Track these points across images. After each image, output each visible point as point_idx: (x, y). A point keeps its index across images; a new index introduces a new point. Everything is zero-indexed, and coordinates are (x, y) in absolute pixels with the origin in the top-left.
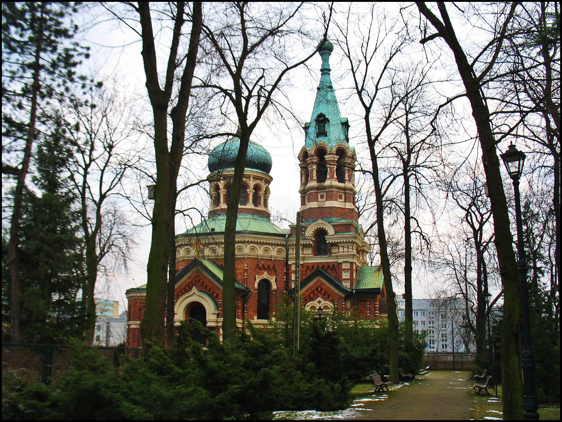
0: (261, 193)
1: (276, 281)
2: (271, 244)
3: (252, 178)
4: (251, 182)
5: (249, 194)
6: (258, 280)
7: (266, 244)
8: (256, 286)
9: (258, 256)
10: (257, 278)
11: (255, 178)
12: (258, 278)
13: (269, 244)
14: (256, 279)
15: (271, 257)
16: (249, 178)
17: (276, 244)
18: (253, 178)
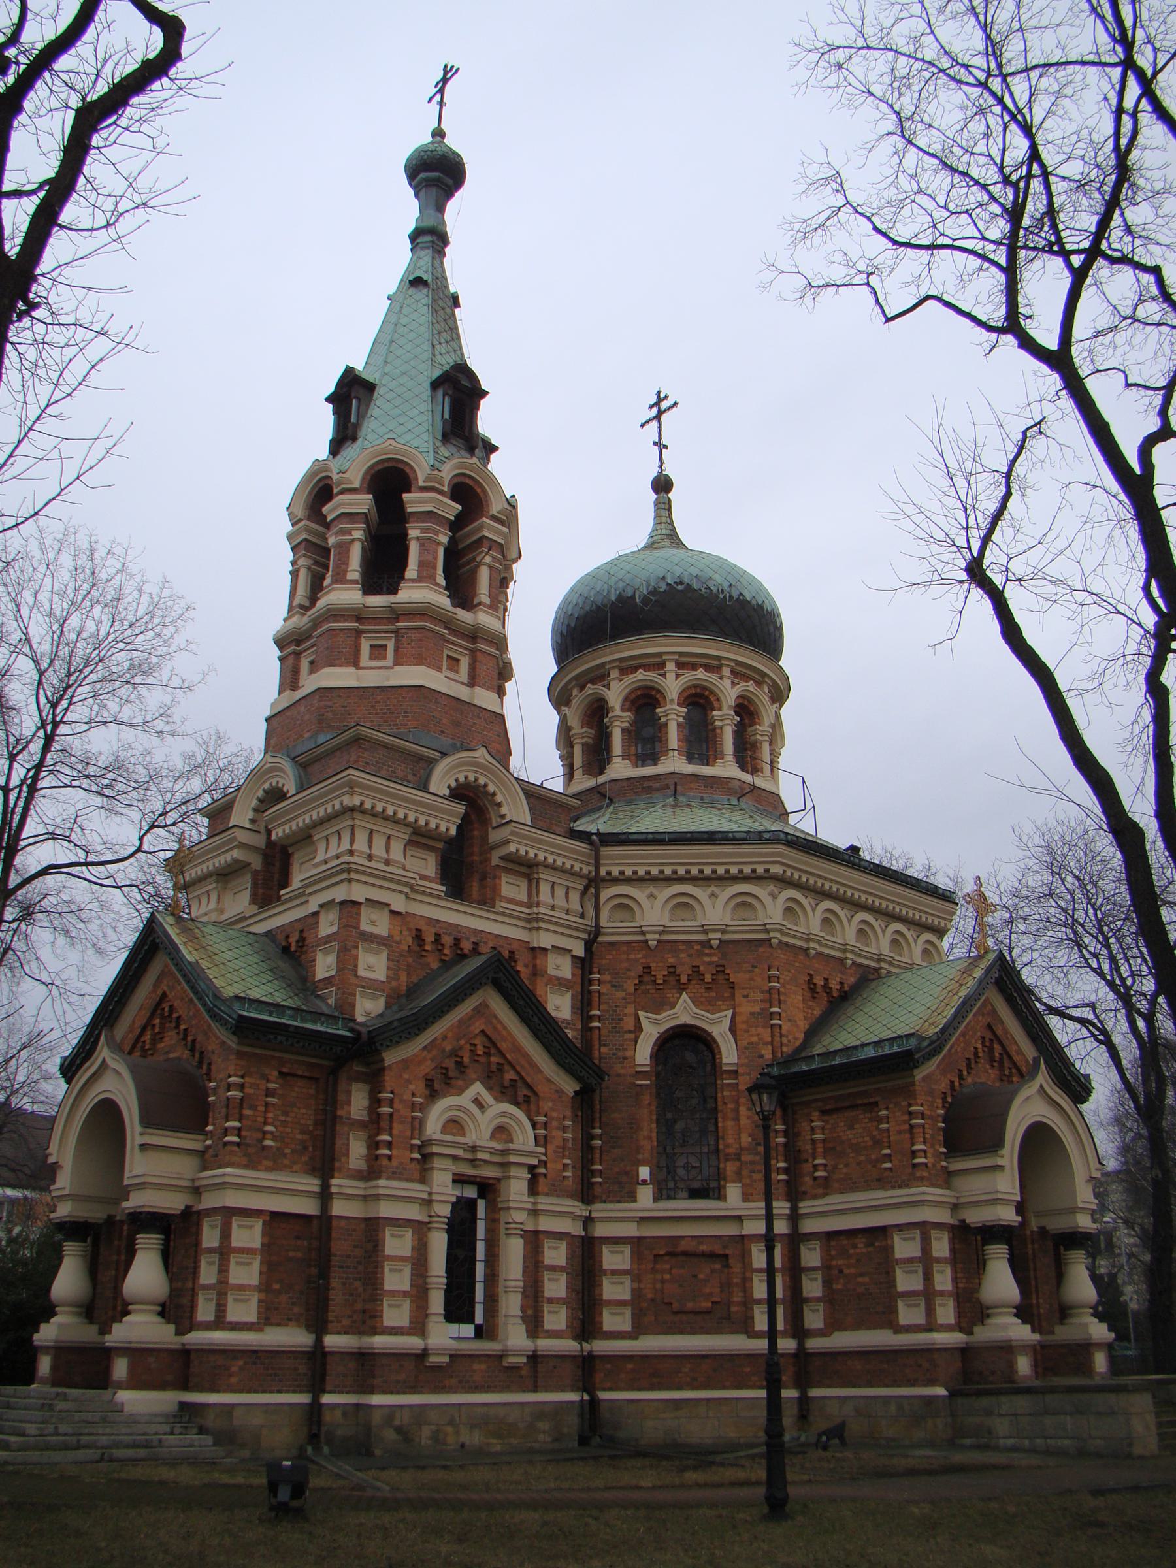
0: (725, 720)
1: (733, 1029)
2: (701, 879)
3: (671, 666)
4: (671, 676)
5: (666, 725)
6: (652, 1029)
7: (676, 879)
8: (643, 1054)
9: (643, 933)
10: (645, 1023)
11: (683, 665)
12: (654, 1022)
13: (688, 879)
14: (639, 1028)
15: (706, 932)
16: (661, 666)
17: (720, 879)
18: (680, 666)
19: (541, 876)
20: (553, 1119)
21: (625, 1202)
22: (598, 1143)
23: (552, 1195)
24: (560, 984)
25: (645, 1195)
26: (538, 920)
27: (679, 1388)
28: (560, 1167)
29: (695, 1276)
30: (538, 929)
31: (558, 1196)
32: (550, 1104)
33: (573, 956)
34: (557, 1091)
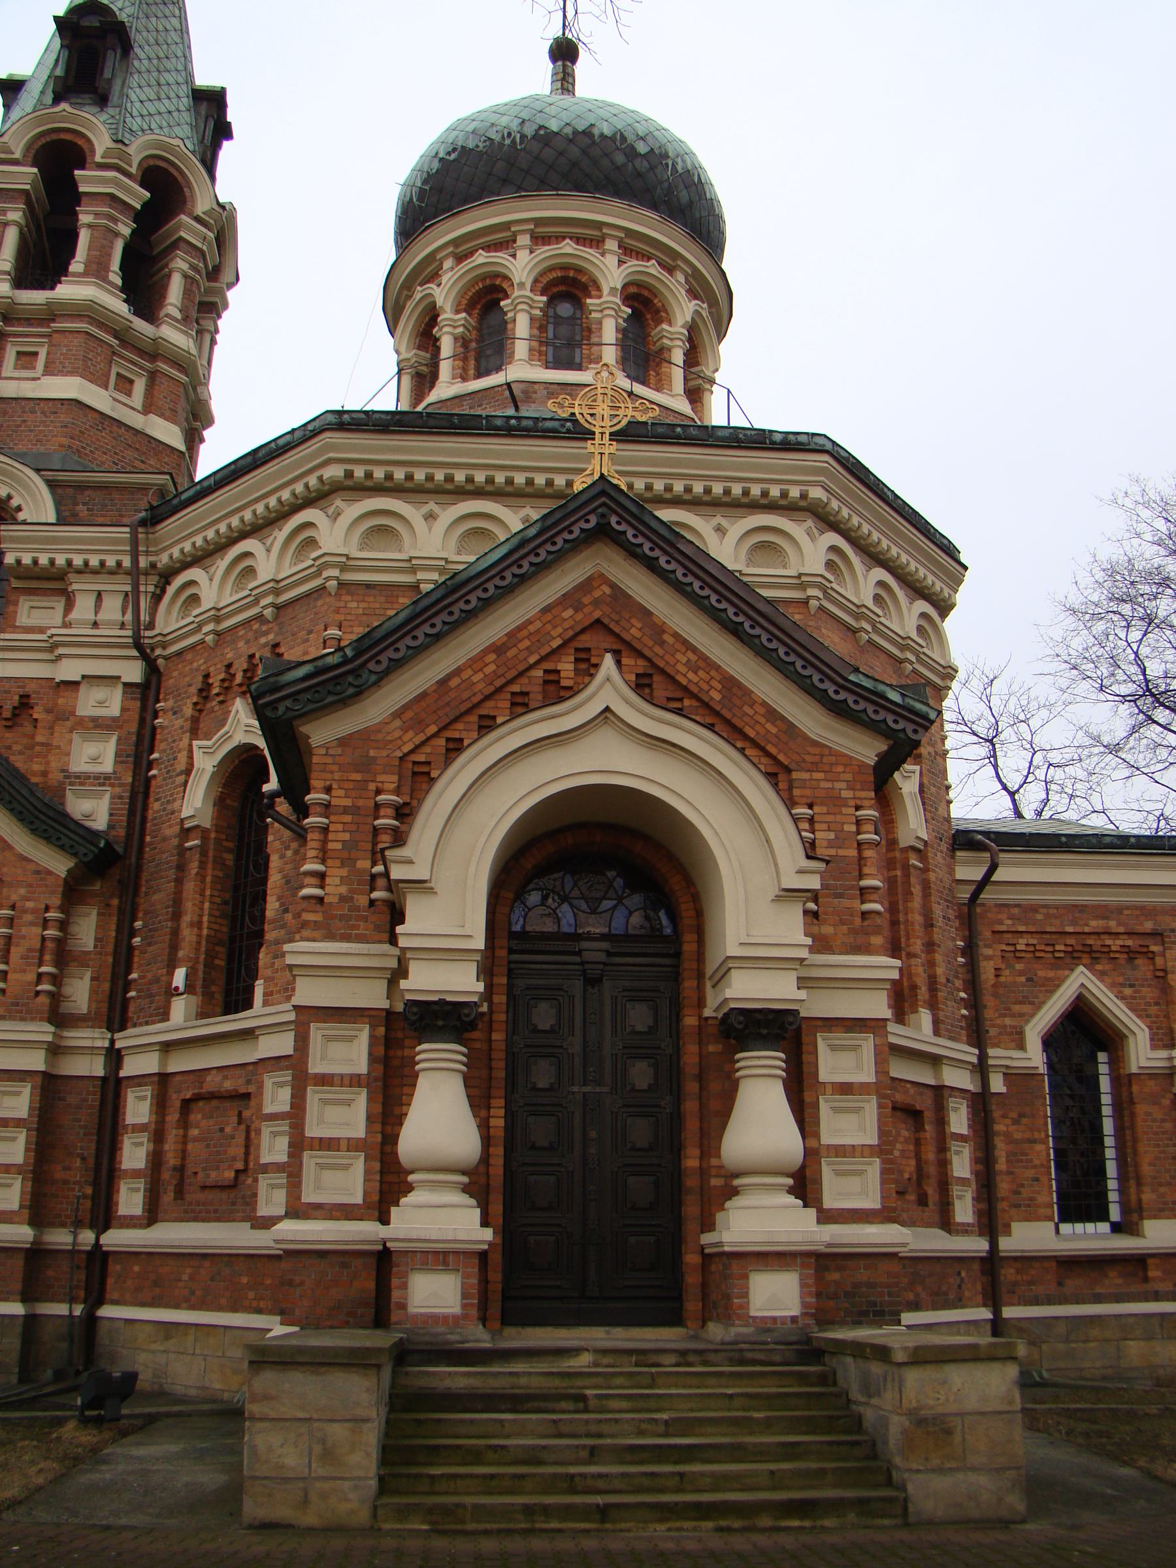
19: (75, 587)
20: (25, 911)
21: (154, 1023)
22: (137, 941)
23: (12, 1018)
24: (97, 727)
25: (179, 1008)
26: (55, 646)
27: (177, 1306)
28: (32, 977)
29: (222, 1130)
30: (60, 657)
31: (22, 1019)
32: (22, 891)
33: (126, 685)
34: (38, 872)
